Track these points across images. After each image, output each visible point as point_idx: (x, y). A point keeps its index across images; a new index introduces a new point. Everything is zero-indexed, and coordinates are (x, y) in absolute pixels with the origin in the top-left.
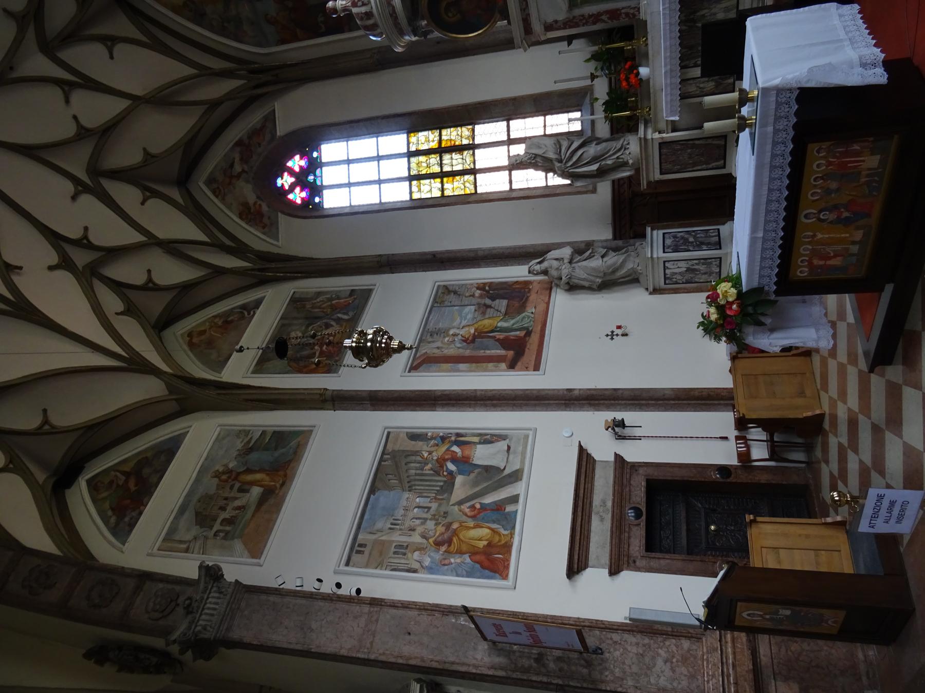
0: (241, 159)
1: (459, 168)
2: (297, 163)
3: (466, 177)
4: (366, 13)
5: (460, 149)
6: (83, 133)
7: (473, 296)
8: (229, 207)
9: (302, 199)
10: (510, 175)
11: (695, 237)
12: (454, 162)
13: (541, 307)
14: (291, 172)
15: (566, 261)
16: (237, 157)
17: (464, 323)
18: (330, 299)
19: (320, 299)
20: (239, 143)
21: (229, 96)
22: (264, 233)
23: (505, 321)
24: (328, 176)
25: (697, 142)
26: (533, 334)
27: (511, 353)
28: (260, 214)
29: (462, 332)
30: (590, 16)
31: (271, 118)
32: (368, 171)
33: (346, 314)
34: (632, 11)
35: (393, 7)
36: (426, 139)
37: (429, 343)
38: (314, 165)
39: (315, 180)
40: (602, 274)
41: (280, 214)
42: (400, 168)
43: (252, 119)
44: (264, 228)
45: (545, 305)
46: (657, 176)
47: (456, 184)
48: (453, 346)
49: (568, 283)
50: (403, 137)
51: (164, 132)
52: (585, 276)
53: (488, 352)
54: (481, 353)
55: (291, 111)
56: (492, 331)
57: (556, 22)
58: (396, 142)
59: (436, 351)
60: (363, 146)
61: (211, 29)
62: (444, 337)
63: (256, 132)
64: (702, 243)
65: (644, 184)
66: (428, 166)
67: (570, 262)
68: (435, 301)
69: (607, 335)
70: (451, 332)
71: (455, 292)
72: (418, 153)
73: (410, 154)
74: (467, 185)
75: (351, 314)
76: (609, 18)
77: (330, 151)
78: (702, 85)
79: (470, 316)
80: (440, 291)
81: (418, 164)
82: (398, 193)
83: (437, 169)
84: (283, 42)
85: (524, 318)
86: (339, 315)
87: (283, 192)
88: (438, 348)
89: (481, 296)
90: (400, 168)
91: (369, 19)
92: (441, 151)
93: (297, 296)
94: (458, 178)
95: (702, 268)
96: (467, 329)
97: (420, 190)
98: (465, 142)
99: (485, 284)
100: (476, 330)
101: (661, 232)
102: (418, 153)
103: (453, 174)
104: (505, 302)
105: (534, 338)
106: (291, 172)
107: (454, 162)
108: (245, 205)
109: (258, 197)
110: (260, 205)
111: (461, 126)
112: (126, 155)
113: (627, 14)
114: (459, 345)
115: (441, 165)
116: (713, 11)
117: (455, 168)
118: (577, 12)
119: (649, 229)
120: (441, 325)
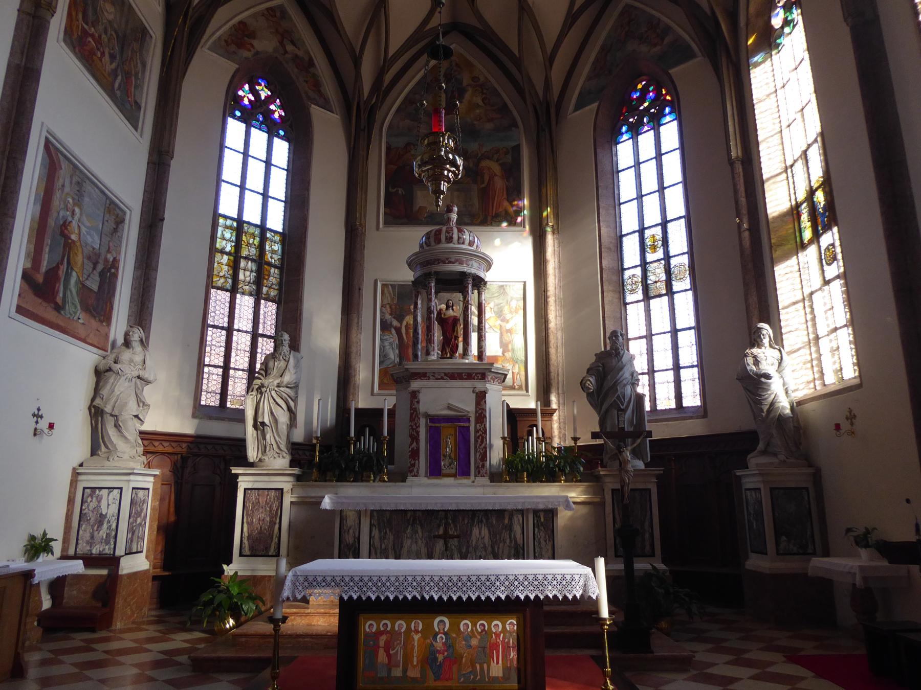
0: (296, 56)
1: (241, 277)
3: (230, 281)
4: (452, 238)
5: (259, 282)
7: (109, 251)
8: (254, 16)
9: (242, 98)
10: (222, 328)
11: (140, 524)
12: (248, 273)
13: (82, 332)
15: (142, 373)
16: (300, 53)
17: (84, 229)
18: (137, 74)
19: (139, 65)
20: (311, 63)
22: (219, 38)
23: (76, 283)
24: (259, 137)
25: (277, 526)
26: (56, 314)
27: (40, 279)
28: (241, 45)
29: (74, 224)
30: (418, 433)
31: (326, 105)
32: (255, 180)
33: (119, 88)
34: (415, 470)
35: (453, 263)
36: (274, 249)
37: (71, 177)
38: (272, 130)
39: (258, 120)
40: (116, 412)
41: (237, 66)
43: (330, 88)
44: (226, 41)
45: (83, 336)
46: (244, 483)
47: (226, 268)
48: (62, 206)
49: (110, 370)
50: (279, 228)
52: (117, 392)
53: (47, 250)
54: (48, 241)
56: (69, 263)
57: (418, 402)
58: (276, 221)
59: (61, 181)
61: (413, 91)
62: (73, 199)
63: (317, 85)
64: (133, 534)
65: (235, 470)
66: (248, 244)
67: (139, 377)
68: (112, 202)
69: (39, 410)
70: (77, 210)
71: (115, 230)
72: (263, 239)
74: (222, 280)
75: (118, 92)
76: (413, 449)
77: (281, 149)
78: (351, 531)
79: (89, 239)
80: (120, 213)
81: (253, 235)
82: (228, 205)
83: (244, 253)
84: (388, 149)
85: (76, 307)
86: (120, 78)
88: (63, 186)
89: (106, 260)
90: (252, 215)
91: (446, 239)
92: (260, 261)
93: (148, 38)
94: (231, 272)
95: (103, 533)
96: (77, 231)
97: (227, 227)
98: (265, 289)
99: (117, 269)
100: (74, 242)
101: (150, 486)
102: (263, 239)
103: (235, 267)
104: (95, 287)
105: (51, 315)
107: (246, 275)
108: (252, 35)
109: (257, 53)
110: (249, 50)
111: (280, 290)
113: (413, 465)
114: (61, 214)
115: (246, 258)
116: (420, 542)
117: (241, 272)
118: (423, 422)
119: (157, 472)
120: (86, 199)
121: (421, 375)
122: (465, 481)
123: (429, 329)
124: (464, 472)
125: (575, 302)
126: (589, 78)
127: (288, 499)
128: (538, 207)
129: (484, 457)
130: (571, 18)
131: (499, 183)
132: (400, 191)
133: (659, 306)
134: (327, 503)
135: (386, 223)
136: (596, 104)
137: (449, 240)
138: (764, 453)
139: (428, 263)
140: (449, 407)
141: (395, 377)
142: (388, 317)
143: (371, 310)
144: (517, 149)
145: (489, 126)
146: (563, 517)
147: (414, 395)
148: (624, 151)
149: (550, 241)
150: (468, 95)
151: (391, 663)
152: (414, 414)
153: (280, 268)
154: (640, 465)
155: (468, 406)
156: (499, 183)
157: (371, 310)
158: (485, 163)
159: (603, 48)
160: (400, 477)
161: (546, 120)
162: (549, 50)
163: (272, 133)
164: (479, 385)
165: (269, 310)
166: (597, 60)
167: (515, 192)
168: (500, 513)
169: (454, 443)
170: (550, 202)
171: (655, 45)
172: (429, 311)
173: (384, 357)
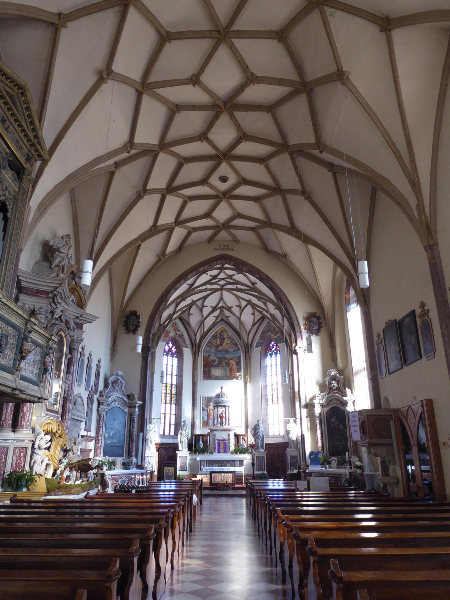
2: (174, 350)
5: (171, 400)
6: (203, 306)
14: (172, 347)
20: (183, 335)
21: (196, 339)
24: (170, 358)
28: (166, 337)
42: (169, 382)
51: (194, 320)
55: (187, 352)
60: (175, 372)
63: (184, 341)
65: (177, 452)
73: (172, 385)
77: (175, 359)
84: (204, 357)
87: (168, 343)
92: (171, 394)
95: (150, 466)
106: (172, 347)
112: (194, 310)
118: (216, 441)
121: (216, 430)
122: (225, 454)
123: (217, 419)
124: (225, 452)
125: (255, 404)
126: (259, 339)
127: (188, 458)
128: (245, 374)
129: (229, 449)
130: (254, 324)
131: (235, 367)
132: (207, 369)
133: (276, 405)
134: (198, 459)
135: (203, 379)
136: (261, 348)
137: (222, 397)
138: (290, 448)
139: (217, 403)
140: (222, 438)
141: (205, 424)
142: (204, 407)
143: (200, 404)
144: (240, 357)
145: (232, 350)
146: (245, 462)
147: (214, 435)
148: (268, 359)
149: (249, 384)
150: (226, 340)
151: (216, 479)
152: (214, 439)
153: (176, 395)
154: (263, 450)
155: (226, 437)
156: (235, 367)
157: (200, 404)
158: (231, 361)
159: (263, 331)
160: (211, 453)
161: (248, 349)
162: (248, 332)
163: (173, 356)
164: (229, 432)
165: (174, 406)
166: (261, 334)
167: (239, 370)
168: (233, 461)
169: (223, 446)
170: (249, 374)
171: (275, 335)
172: (217, 414)
173: (203, 418)
